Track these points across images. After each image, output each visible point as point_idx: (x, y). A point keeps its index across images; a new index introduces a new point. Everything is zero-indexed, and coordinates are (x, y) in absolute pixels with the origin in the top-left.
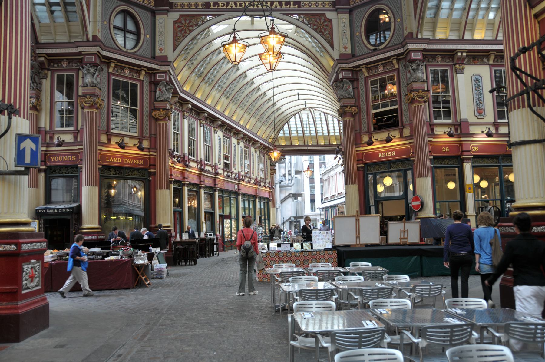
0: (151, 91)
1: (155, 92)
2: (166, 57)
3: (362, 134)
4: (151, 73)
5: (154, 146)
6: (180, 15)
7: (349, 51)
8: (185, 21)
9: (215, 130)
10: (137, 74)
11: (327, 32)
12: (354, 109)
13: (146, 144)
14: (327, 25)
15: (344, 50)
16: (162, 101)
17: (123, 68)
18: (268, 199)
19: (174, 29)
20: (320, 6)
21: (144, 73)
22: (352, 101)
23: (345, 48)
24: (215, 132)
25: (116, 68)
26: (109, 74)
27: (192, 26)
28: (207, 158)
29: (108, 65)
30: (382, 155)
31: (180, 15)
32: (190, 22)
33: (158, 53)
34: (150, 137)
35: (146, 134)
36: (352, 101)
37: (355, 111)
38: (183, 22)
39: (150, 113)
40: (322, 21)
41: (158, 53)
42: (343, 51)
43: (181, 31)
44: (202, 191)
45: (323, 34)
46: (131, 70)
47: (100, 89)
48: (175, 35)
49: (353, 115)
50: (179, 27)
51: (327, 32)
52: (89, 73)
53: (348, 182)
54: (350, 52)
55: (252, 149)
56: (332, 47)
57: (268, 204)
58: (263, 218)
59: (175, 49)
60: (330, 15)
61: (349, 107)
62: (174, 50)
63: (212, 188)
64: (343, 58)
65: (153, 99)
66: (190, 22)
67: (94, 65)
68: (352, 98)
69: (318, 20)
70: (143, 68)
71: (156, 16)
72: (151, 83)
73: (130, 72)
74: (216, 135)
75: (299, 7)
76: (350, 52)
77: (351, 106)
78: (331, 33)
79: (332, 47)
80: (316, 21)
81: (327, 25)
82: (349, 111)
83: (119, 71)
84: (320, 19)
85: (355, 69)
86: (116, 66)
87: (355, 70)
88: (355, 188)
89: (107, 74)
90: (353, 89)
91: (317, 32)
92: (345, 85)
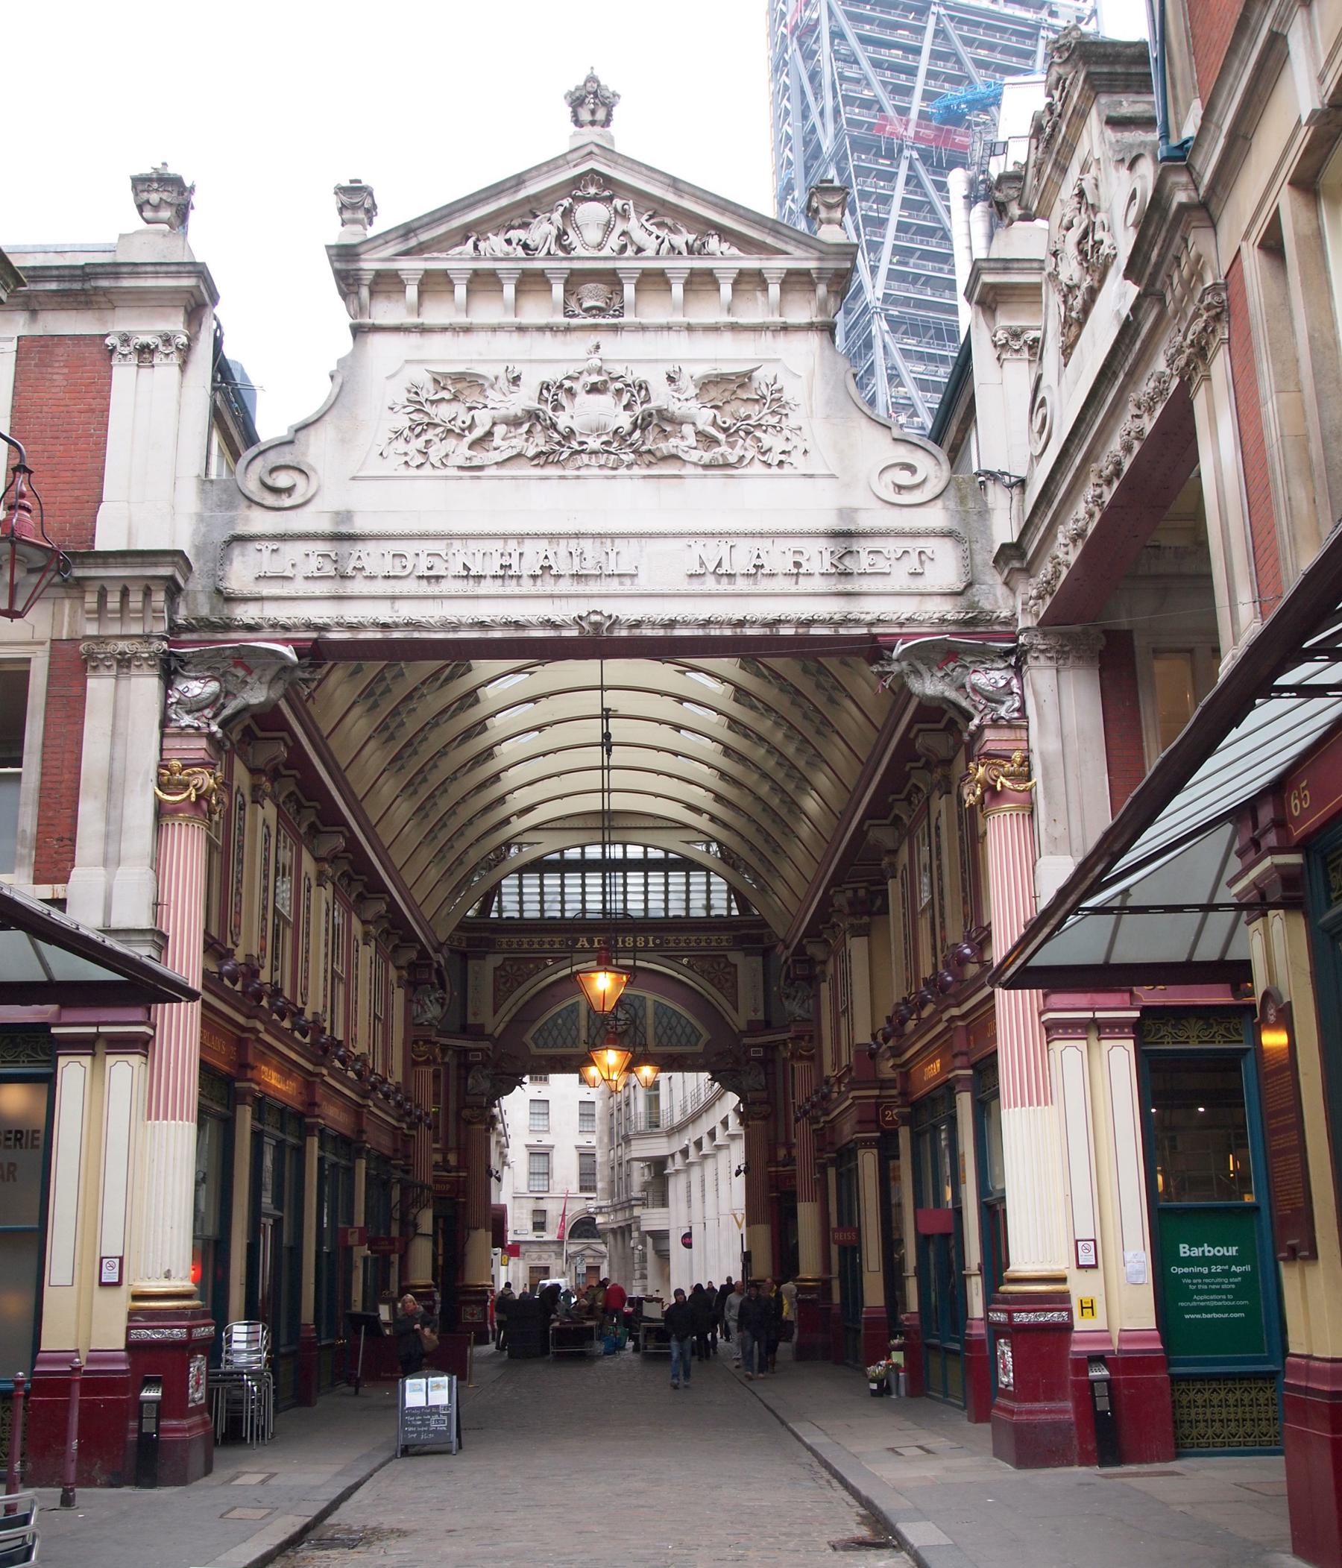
1: (466, 1079)
2: (482, 1026)
4: (463, 1052)
6: (505, 959)
7: (760, 1016)
11: (729, 984)
21: (450, 1052)
22: (764, 1095)
23: (755, 1011)
33: (471, 1020)
36: (764, 1095)
39: (458, 1114)
41: (471, 1020)
42: (752, 1016)
48: (496, 989)
49: (765, 1118)
51: (729, 984)
56: (736, 1009)
59: (495, 1012)
60: (735, 957)
62: (495, 1012)
64: (754, 1028)
71: (471, 963)
72: (459, 1066)
77: (762, 1103)
78: (735, 985)
79: (736, 1009)
90: (766, 1074)
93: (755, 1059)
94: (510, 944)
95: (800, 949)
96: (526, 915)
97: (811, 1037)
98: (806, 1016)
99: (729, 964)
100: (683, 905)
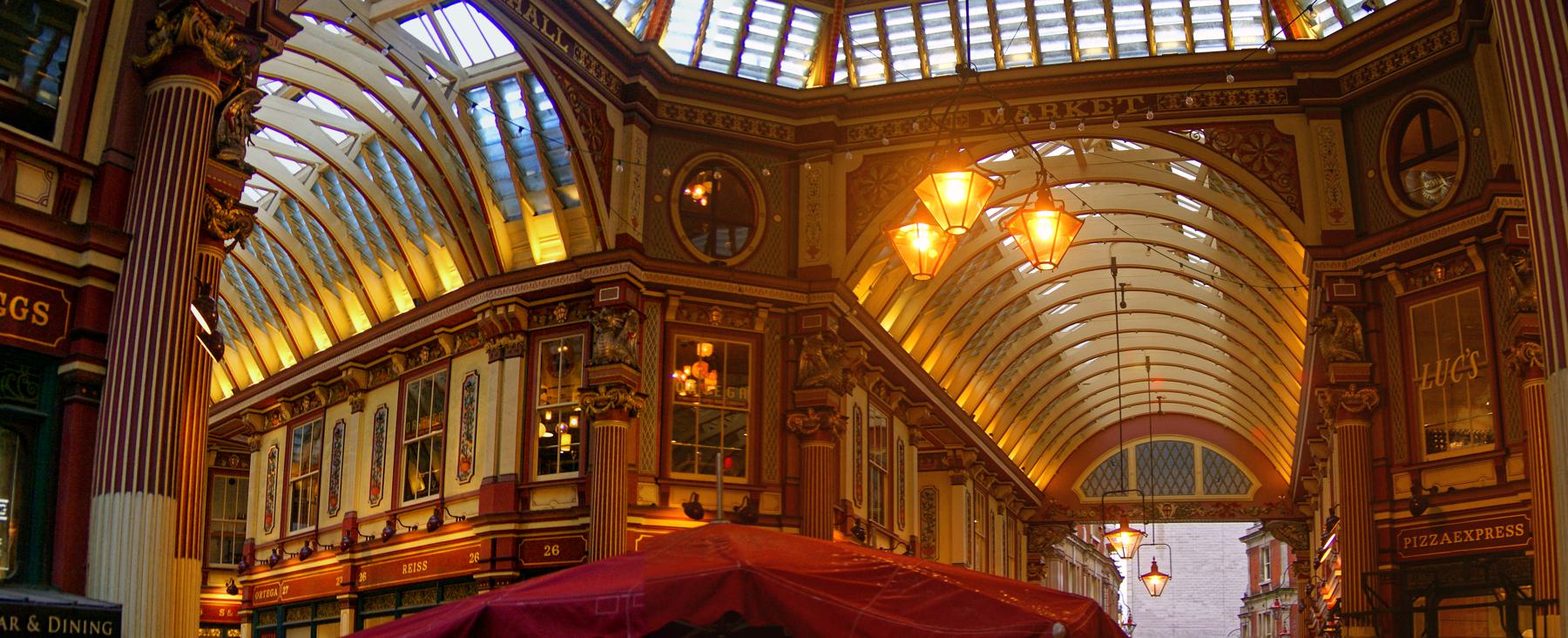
3: (1392, 470)
6: (865, 157)
7: (1348, 223)
10: (747, 320)
12: (1368, 395)
14: (1281, 152)
15: (1333, 220)
17: (705, 310)
23: (1337, 214)
25: (686, 308)
26: (666, 328)
29: (664, 303)
30: (1494, 533)
31: (865, 157)
33: (805, 261)
37: (1370, 399)
41: (805, 261)
42: (1330, 225)
45: (1271, 177)
46: (728, 312)
47: (637, 369)
49: (1366, 415)
52: (606, 329)
54: (1350, 226)
61: (1352, 387)
67: (620, 308)
68: (1362, 361)
70: (760, 304)
73: (725, 316)
76: (1350, 226)
77: (1359, 386)
78: (1293, 175)
80: (1248, 141)
81: (1281, 152)
82: (1353, 398)
83: (695, 316)
84: (1260, 136)
85: (1368, 275)
86: (683, 305)
87: (1369, 278)
89: (658, 330)
90: (1365, 333)
91: (1252, 172)
92: (1340, 324)
93: (1340, 301)
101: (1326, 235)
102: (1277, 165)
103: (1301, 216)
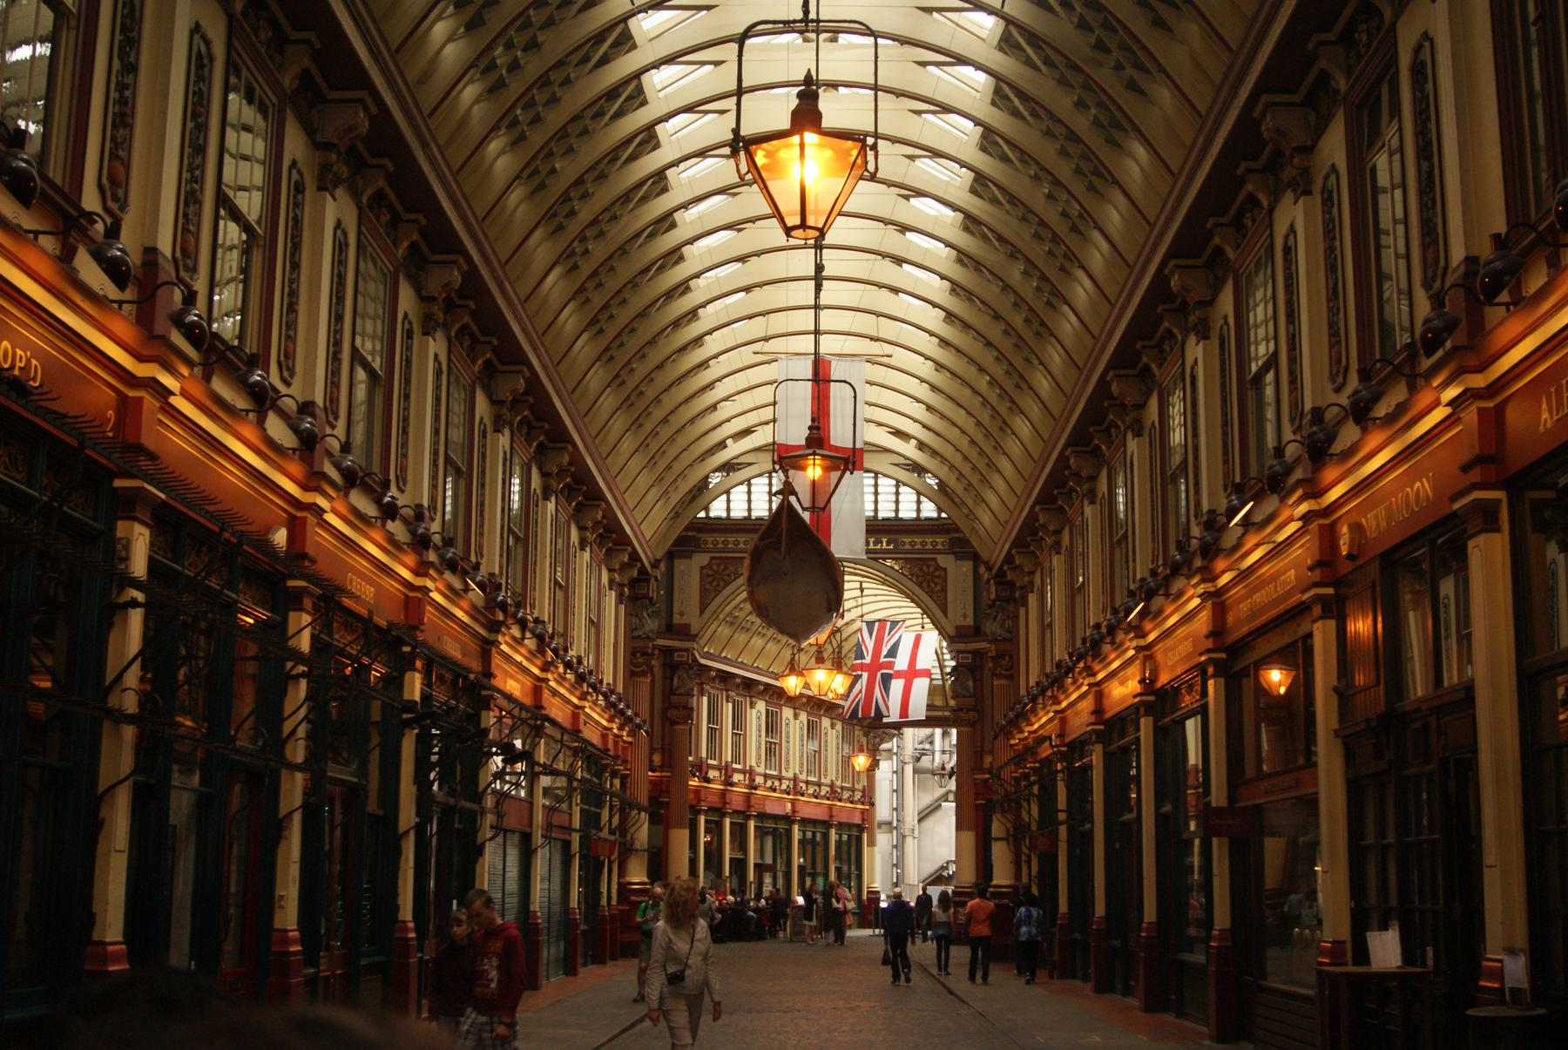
0: (665, 678)
1: (672, 679)
2: (688, 626)
4: (667, 652)
5: (668, 763)
6: (712, 558)
7: (970, 621)
8: (718, 565)
9: (751, 703)
13: (657, 759)
14: (938, 577)
16: (681, 694)
18: (861, 828)
19: (701, 580)
20: (929, 547)
22: (970, 702)
23: (965, 616)
24: (752, 705)
27: (729, 575)
28: (736, 759)
31: (712, 558)
32: (726, 568)
33: (677, 619)
34: (663, 749)
35: (657, 745)
38: (715, 567)
40: (932, 569)
41: (677, 619)
42: (961, 622)
43: (711, 582)
44: (727, 821)
48: (703, 590)
49: (972, 724)
50: (709, 575)
53: (959, 827)
54: (972, 623)
55: (826, 722)
57: (859, 840)
58: (845, 868)
59: (702, 612)
60: (944, 561)
62: (702, 612)
63: (742, 812)
65: (669, 692)
66: (726, 568)
69: (925, 568)
71: (677, 562)
72: (664, 665)
74: (754, 711)
75: (896, 542)
77: (968, 710)
78: (944, 590)
80: (921, 569)
81: (938, 577)
84: (928, 566)
88: (970, 836)
90: (974, 681)
94: (715, 543)
95: (1001, 574)
96: (733, 514)
97: (1011, 658)
98: (1006, 635)
99: (938, 568)
100: (893, 506)
101: (958, 628)
102: (936, 584)
103: (946, 615)
